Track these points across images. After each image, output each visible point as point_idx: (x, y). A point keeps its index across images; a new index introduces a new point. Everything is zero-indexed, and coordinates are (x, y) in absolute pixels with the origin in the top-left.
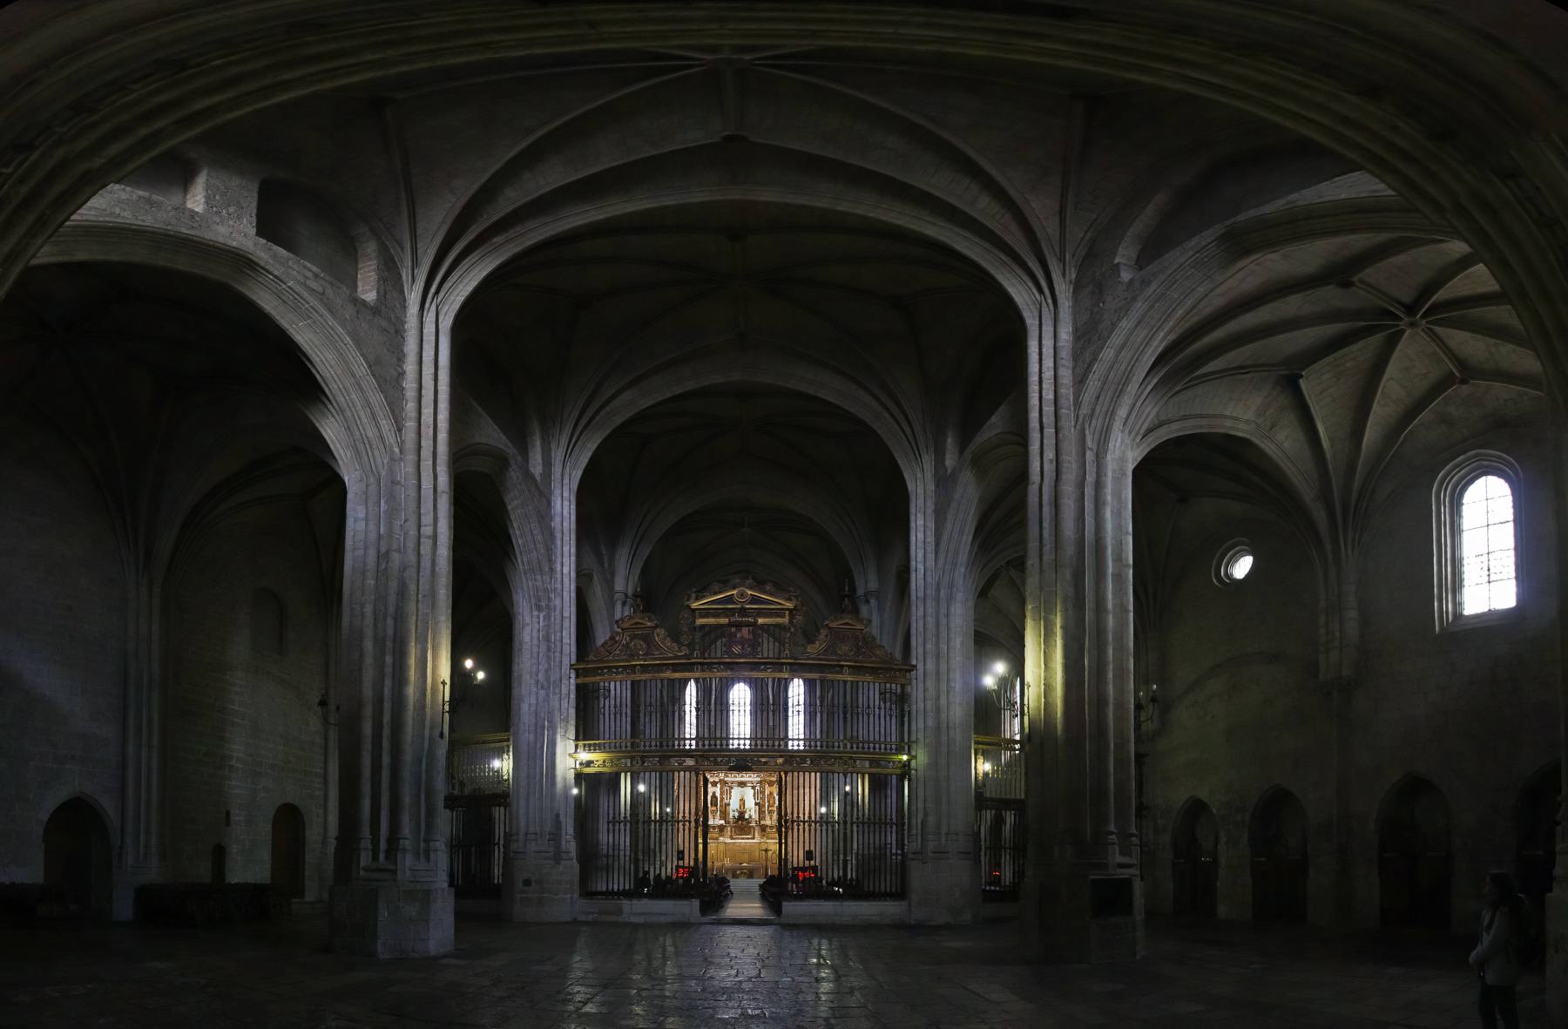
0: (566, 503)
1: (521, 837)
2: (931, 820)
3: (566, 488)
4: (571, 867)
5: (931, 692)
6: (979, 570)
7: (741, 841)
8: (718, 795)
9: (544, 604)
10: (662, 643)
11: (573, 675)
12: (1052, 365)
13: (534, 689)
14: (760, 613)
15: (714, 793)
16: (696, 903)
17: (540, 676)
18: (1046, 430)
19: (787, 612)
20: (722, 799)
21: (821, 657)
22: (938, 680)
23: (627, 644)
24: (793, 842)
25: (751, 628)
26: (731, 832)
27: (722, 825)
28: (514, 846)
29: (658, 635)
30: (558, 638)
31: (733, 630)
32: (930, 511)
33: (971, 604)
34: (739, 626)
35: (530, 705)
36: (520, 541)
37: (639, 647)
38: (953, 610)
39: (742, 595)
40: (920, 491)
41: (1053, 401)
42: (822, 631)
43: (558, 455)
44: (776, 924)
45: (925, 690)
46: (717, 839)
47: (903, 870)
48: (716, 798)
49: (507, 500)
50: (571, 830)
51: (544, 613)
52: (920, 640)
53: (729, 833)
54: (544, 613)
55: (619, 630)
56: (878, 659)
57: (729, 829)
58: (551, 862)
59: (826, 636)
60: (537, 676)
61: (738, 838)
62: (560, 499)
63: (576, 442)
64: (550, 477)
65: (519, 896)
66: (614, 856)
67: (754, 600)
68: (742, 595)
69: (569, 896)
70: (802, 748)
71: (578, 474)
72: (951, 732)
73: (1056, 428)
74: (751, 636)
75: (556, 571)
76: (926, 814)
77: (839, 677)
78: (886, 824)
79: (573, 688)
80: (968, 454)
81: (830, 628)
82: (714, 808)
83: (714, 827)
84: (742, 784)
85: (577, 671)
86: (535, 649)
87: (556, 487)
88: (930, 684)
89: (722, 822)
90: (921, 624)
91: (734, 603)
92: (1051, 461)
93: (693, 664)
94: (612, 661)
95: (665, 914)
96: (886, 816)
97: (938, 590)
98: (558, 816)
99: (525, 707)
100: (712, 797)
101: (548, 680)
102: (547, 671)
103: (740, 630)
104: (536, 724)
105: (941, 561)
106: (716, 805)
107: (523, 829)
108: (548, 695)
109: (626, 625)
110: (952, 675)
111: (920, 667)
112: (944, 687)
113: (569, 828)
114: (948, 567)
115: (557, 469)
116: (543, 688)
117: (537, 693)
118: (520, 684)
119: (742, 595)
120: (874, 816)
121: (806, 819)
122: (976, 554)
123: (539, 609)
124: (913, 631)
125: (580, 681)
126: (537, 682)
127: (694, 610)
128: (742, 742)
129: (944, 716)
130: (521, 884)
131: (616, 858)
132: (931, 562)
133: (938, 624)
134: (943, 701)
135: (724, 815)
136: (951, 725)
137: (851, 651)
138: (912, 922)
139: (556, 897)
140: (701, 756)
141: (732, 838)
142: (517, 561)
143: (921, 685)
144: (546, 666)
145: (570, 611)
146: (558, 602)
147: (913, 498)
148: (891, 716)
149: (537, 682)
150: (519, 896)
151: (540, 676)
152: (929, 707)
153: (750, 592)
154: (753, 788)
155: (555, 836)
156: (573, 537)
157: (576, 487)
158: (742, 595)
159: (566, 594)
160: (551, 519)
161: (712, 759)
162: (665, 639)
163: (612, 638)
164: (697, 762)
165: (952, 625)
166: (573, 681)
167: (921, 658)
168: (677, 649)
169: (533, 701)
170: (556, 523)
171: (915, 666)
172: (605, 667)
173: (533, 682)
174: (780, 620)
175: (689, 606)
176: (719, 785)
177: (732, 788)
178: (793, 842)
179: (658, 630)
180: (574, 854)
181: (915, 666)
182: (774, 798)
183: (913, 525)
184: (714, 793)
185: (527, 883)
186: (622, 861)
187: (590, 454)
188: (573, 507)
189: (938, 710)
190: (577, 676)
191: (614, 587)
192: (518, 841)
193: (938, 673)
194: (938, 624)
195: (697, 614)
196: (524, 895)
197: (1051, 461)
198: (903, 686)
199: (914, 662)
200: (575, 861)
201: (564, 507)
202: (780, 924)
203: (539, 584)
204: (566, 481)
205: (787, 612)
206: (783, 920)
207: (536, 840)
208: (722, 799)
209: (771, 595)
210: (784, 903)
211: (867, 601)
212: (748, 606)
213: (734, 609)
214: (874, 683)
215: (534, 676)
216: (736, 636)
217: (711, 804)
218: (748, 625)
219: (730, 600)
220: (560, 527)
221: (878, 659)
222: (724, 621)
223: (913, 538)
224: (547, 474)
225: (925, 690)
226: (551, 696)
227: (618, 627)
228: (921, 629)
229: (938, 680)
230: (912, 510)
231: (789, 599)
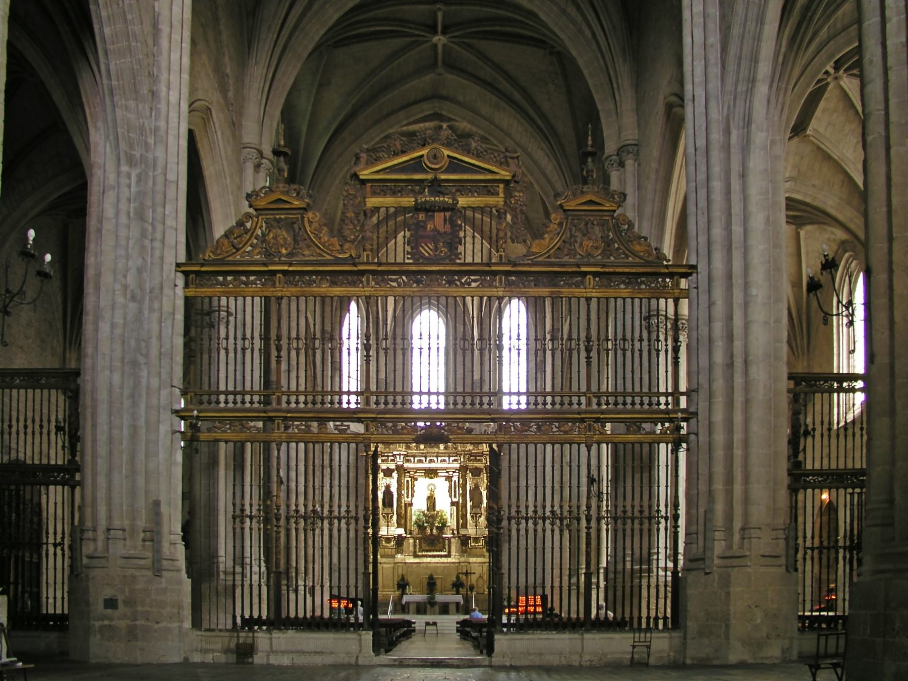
1: (101, 536)
7: (429, 560)
8: (394, 489)
9: (138, 156)
11: (180, 281)
13: (120, 300)
14: (464, 188)
15: (388, 487)
16: (368, 636)
17: (131, 280)
19: (502, 186)
20: (400, 496)
21: (553, 260)
23: (264, 235)
25: (448, 214)
26: (415, 546)
27: (400, 536)
28: (88, 548)
29: (310, 222)
30: (159, 217)
31: (421, 216)
34: (429, 209)
35: (113, 326)
37: (282, 242)
39: (435, 157)
42: (553, 216)
45: (711, 304)
46: (393, 557)
48: (391, 494)
51: (138, 171)
53: (412, 549)
55: (251, 210)
56: (638, 260)
57: (411, 541)
58: (150, 573)
59: (561, 224)
60: (125, 276)
61: (426, 556)
65: (97, 624)
67: (455, 166)
70: (523, 406)
74: (448, 228)
77: (577, 291)
79: (180, 303)
81: (565, 211)
82: (388, 510)
83: (388, 540)
84: (431, 473)
85: (186, 274)
89: (401, 531)
91: (423, 171)
93: (362, 273)
95: (321, 653)
98: (157, 504)
100: (384, 493)
101: (141, 286)
102: (140, 271)
104: (123, 358)
106: (391, 506)
107: (102, 523)
108: (140, 311)
109: (262, 204)
111: (702, 268)
112: (738, 297)
116: (133, 298)
125: (191, 292)
126: (125, 287)
127: (363, 182)
128: (434, 398)
135: (402, 521)
137: (597, 248)
139: (156, 626)
140: (375, 419)
141: (415, 556)
144: (139, 262)
149: (125, 287)
150: (97, 624)
153: (446, 152)
154: (449, 479)
155: (154, 536)
159: (171, 140)
161: (390, 425)
162: (320, 231)
163: (240, 224)
164: (367, 429)
166: (180, 291)
167: (703, 251)
168: (338, 248)
169: (119, 320)
171: (694, 267)
173: (118, 287)
174: (491, 200)
175: (355, 176)
176: (395, 475)
177: (416, 479)
179: (310, 214)
181: (694, 267)
182: (481, 493)
184: (388, 487)
185: (111, 603)
190: (187, 285)
191: (241, 137)
192: (95, 540)
195: (368, 189)
196: (106, 622)
205: (502, 186)
207: (125, 539)
208: (400, 496)
209: (478, 156)
210: (496, 637)
211: (622, 164)
212: (443, 177)
213: (422, 181)
214: (633, 299)
215: (120, 277)
216: (425, 228)
217: (384, 504)
218: (444, 209)
219: (417, 165)
221: (638, 260)
222: (408, 201)
226: (146, 312)
227: (251, 206)
231: (504, 164)
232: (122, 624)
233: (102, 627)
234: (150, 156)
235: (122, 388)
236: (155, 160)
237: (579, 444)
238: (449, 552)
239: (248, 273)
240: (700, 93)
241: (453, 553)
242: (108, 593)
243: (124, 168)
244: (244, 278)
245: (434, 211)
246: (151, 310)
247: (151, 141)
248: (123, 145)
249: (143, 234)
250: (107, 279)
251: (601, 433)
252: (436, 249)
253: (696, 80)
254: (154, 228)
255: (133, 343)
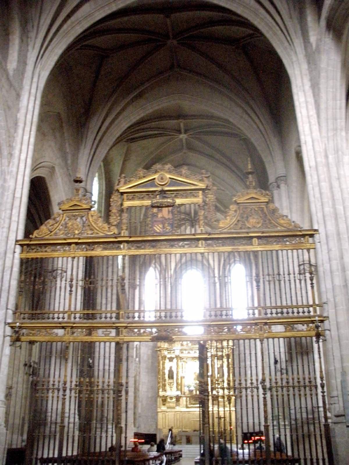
5: (335, 253)
10: (95, 223)
14: (178, 193)
21: (233, 231)
25: (170, 208)
31: (155, 210)
38: (342, 172)
39: (162, 178)
42: (231, 207)
45: (329, 250)
52: (319, 204)
56: (283, 228)
59: (236, 211)
67: (174, 182)
77: (249, 248)
81: (238, 203)
88: (333, 244)
90: (317, 189)
91: (156, 186)
97: (326, 157)
103: (161, 211)
109: (66, 207)
111: (322, 230)
119: (162, 178)
127: (122, 194)
133: (331, 188)
137: (258, 223)
143: (325, 247)
152: (334, 267)
153: (168, 176)
167: (321, 221)
175: (118, 190)
194: (331, 188)
205: (201, 192)
209: (187, 177)
213: (155, 191)
221: (283, 228)
222: (147, 202)
225: (329, 250)
228: (318, 195)
231: (201, 180)
237: (255, 339)
251: (269, 332)
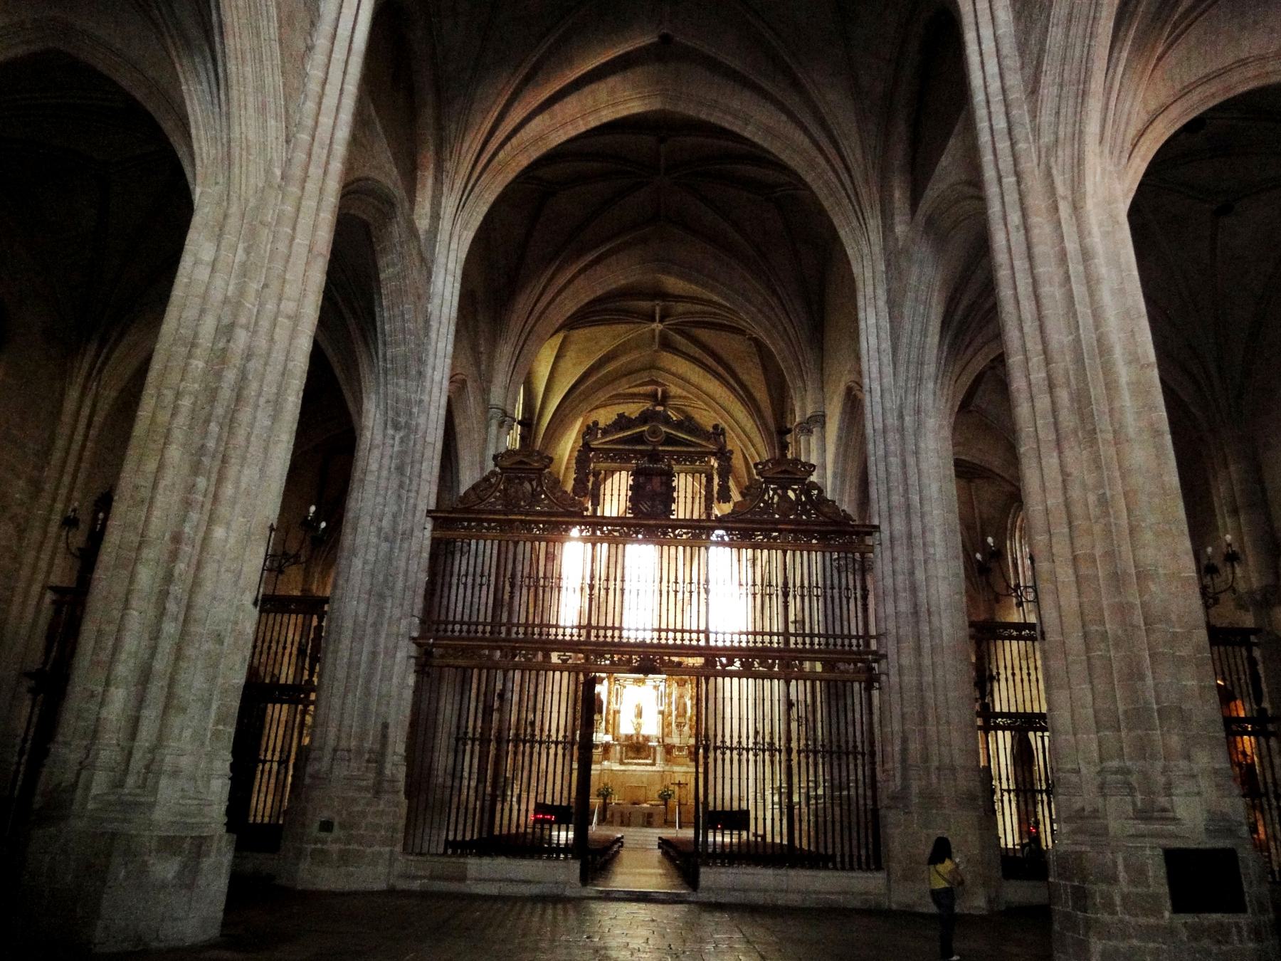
0: (450, 278)
1: (327, 759)
2: (914, 747)
3: (452, 256)
4: (395, 806)
5: (902, 564)
6: (952, 383)
11: (429, 526)
12: (996, 70)
13: (374, 540)
16: (576, 866)
18: (1005, 180)
22: (910, 546)
24: (715, 778)
32: (881, 303)
33: (947, 433)
35: (365, 562)
36: (387, 327)
39: (654, 432)
40: (868, 274)
41: (1006, 131)
43: (449, 204)
44: (689, 903)
47: (875, 822)
49: (382, 263)
50: (401, 748)
52: (883, 489)
54: (402, 434)
60: (381, 520)
62: (443, 271)
63: (467, 199)
64: (435, 237)
66: (452, 787)
68: (654, 432)
69: (388, 849)
71: (469, 235)
72: (935, 619)
73: (1020, 193)
75: (425, 377)
76: (905, 740)
78: (847, 754)
79: (427, 543)
80: (920, 218)
86: (383, 483)
87: (440, 249)
88: (901, 551)
90: (882, 466)
92: (1017, 228)
94: (482, 512)
96: (847, 742)
98: (385, 726)
99: (358, 563)
101: (395, 531)
105: (902, 377)
107: (331, 742)
108: (391, 549)
110: (929, 537)
111: (885, 527)
112: (919, 555)
113: (398, 745)
114: (912, 384)
115: (445, 225)
116: (386, 540)
117: (377, 546)
118: (355, 529)
119: (654, 432)
120: (831, 741)
121: (735, 744)
122: (946, 358)
123: (396, 427)
124: (872, 477)
125: (438, 534)
129: (922, 596)
130: (316, 825)
131: (456, 792)
132: (888, 380)
133: (904, 464)
134: (920, 575)
136: (934, 609)
138: (894, 907)
142: (377, 353)
143: (887, 554)
144: (395, 508)
145: (435, 436)
146: (422, 420)
147: (860, 285)
148: (848, 599)
149: (380, 530)
151: (385, 523)
152: (900, 585)
153: (664, 429)
155: (379, 758)
156: (452, 328)
157: (464, 256)
158: (654, 432)
160: (429, 299)
165: (924, 466)
169: (371, 557)
170: (433, 307)
172: (473, 520)
173: (373, 529)
178: (715, 778)
180: (401, 785)
181: (877, 528)
183: (862, 325)
185: (327, 826)
186: (464, 797)
187: (485, 209)
188: (458, 285)
189: (914, 589)
193: (910, 536)
194: (904, 464)
196: (319, 846)
197: (1017, 228)
198: (862, 555)
199: (876, 522)
200: (402, 794)
201: (447, 283)
202: (696, 903)
203: (401, 391)
204: (454, 246)
206: (702, 896)
207: (349, 760)
210: (702, 870)
215: (376, 521)
220: (438, 313)
223: (864, 345)
224: (433, 231)
225: (894, 560)
228: (882, 474)
229: (910, 546)
230: (861, 303)
232: (335, 847)
233: (314, 850)
234: (414, 423)
235: (366, 616)
236: (417, 425)
238: (654, 760)
239: (489, 521)
240: (876, 386)
241: (658, 761)
242: (325, 815)
243: (390, 432)
244: (485, 524)
245: (652, 475)
246: (401, 549)
247: (415, 410)
248: (390, 413)
249: (401, 486)
250: (365, 521)
252: (652, 507)
253: (872, 376)
254: (411, 480)
255: (381, 578)
